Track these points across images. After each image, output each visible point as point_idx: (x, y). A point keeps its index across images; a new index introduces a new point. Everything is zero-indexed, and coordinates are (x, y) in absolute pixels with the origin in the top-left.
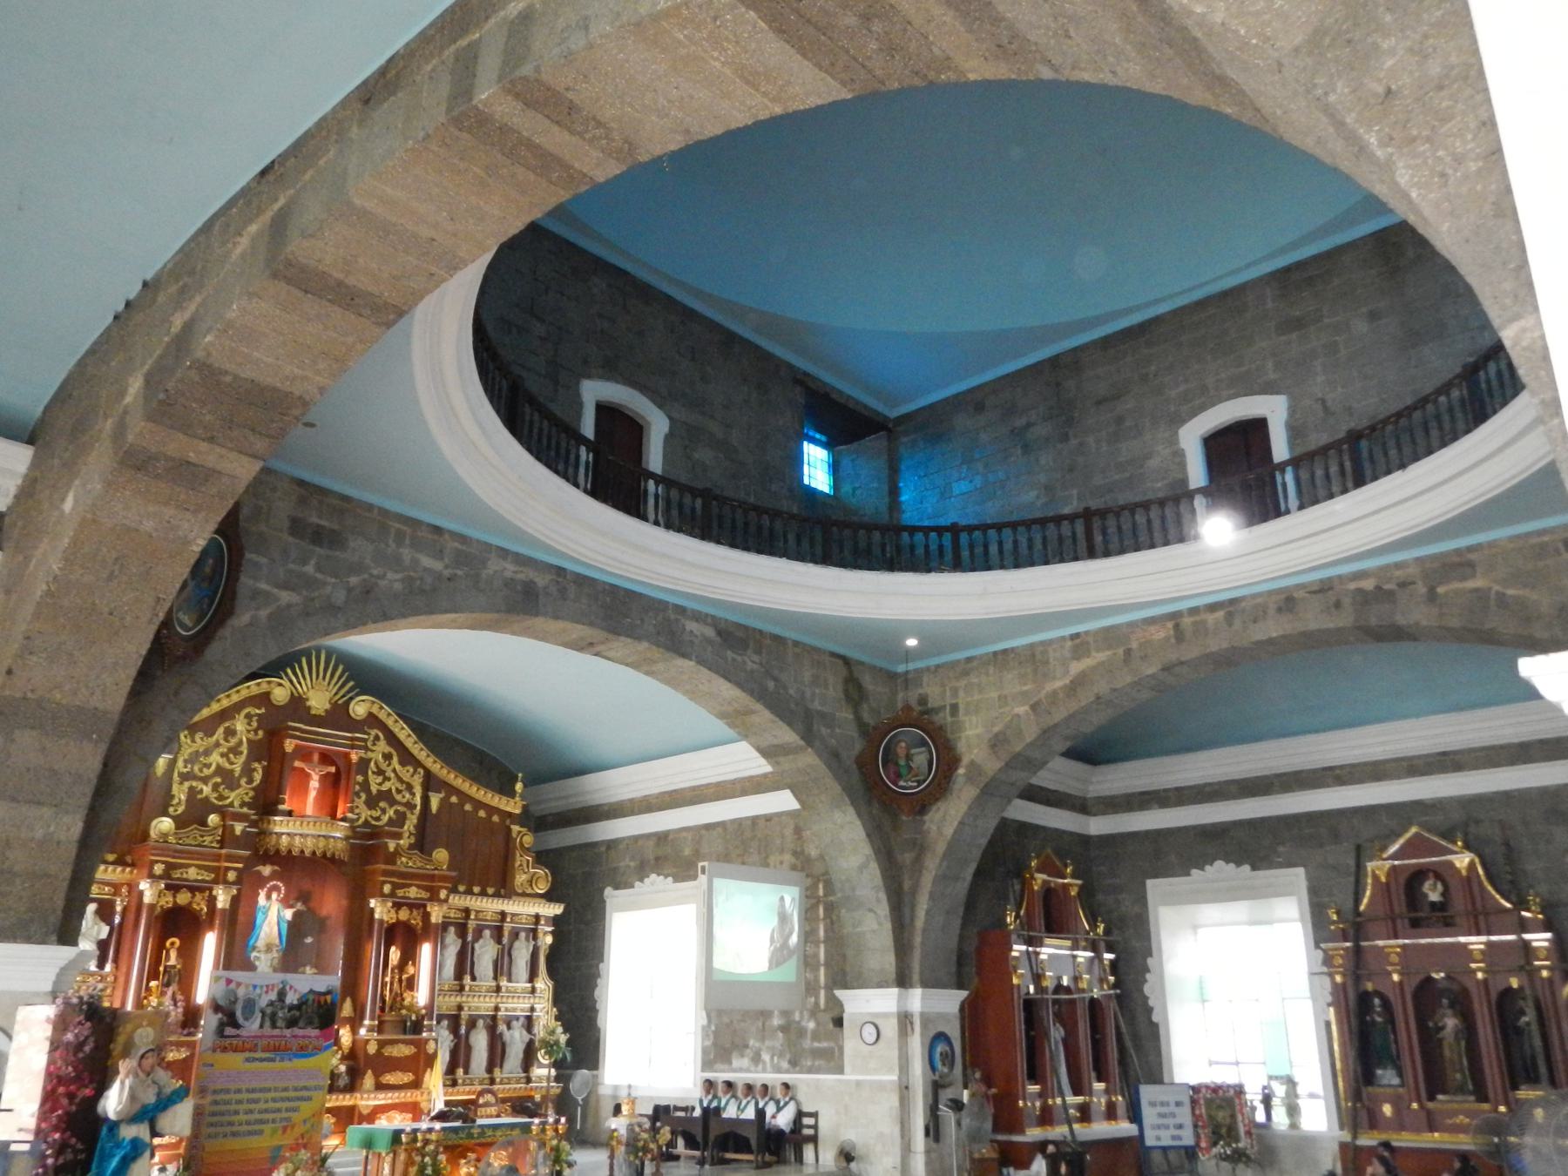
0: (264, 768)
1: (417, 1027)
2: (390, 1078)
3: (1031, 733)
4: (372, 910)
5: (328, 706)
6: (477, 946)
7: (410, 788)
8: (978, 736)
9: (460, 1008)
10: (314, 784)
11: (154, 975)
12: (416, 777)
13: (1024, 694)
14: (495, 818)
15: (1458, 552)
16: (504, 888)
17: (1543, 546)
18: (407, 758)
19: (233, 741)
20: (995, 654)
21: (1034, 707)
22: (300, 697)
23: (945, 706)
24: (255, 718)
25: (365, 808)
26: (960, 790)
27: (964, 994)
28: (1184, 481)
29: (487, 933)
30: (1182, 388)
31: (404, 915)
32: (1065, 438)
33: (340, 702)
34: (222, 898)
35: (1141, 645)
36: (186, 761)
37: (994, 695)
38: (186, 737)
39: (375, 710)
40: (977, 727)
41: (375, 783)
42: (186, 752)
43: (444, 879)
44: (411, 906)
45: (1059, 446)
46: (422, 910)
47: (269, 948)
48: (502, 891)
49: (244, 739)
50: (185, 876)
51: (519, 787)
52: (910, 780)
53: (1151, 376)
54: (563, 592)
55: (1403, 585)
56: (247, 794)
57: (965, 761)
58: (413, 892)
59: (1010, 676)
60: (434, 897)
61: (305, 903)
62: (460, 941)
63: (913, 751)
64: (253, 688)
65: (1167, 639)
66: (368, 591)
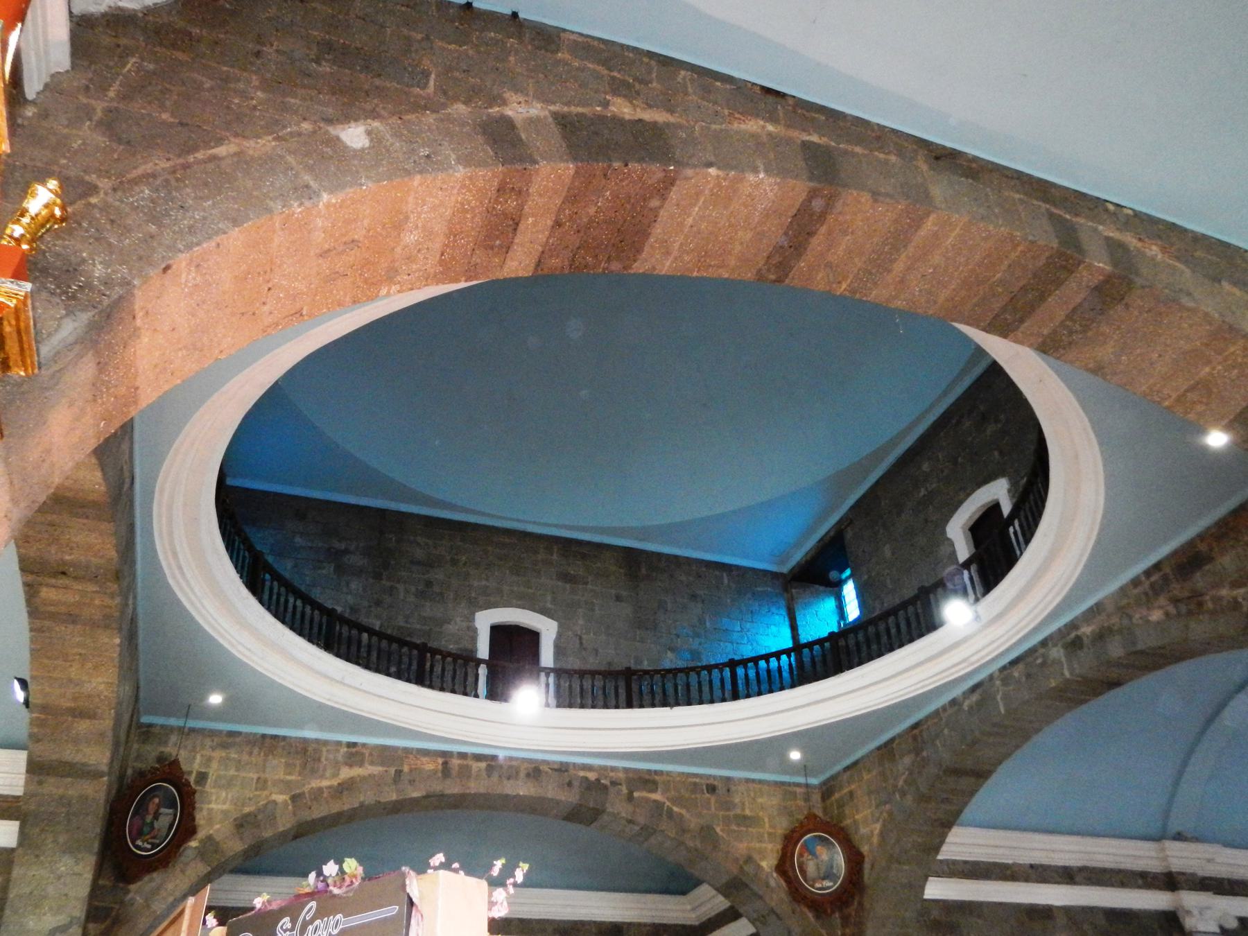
3: (285, 823)
8: (222, 811)
13: (288, 784)
15: (649, 772)
17: (695, 784)
20: (264, 736)
21: (294, 798)
23: (192, 772)
26: (187, 864)
28: (474, 651)
30: (484, 583)
32: (378, 577)
35: (411, 770)
37: (255, 776)
40: (224, 803)
45: (371, 581)
52: (147, 841)
53: (461, 564)
55: (614, 783)
57: (201, 834)
59: (275, 762)
63: (163, 810)
65: (435, 772)
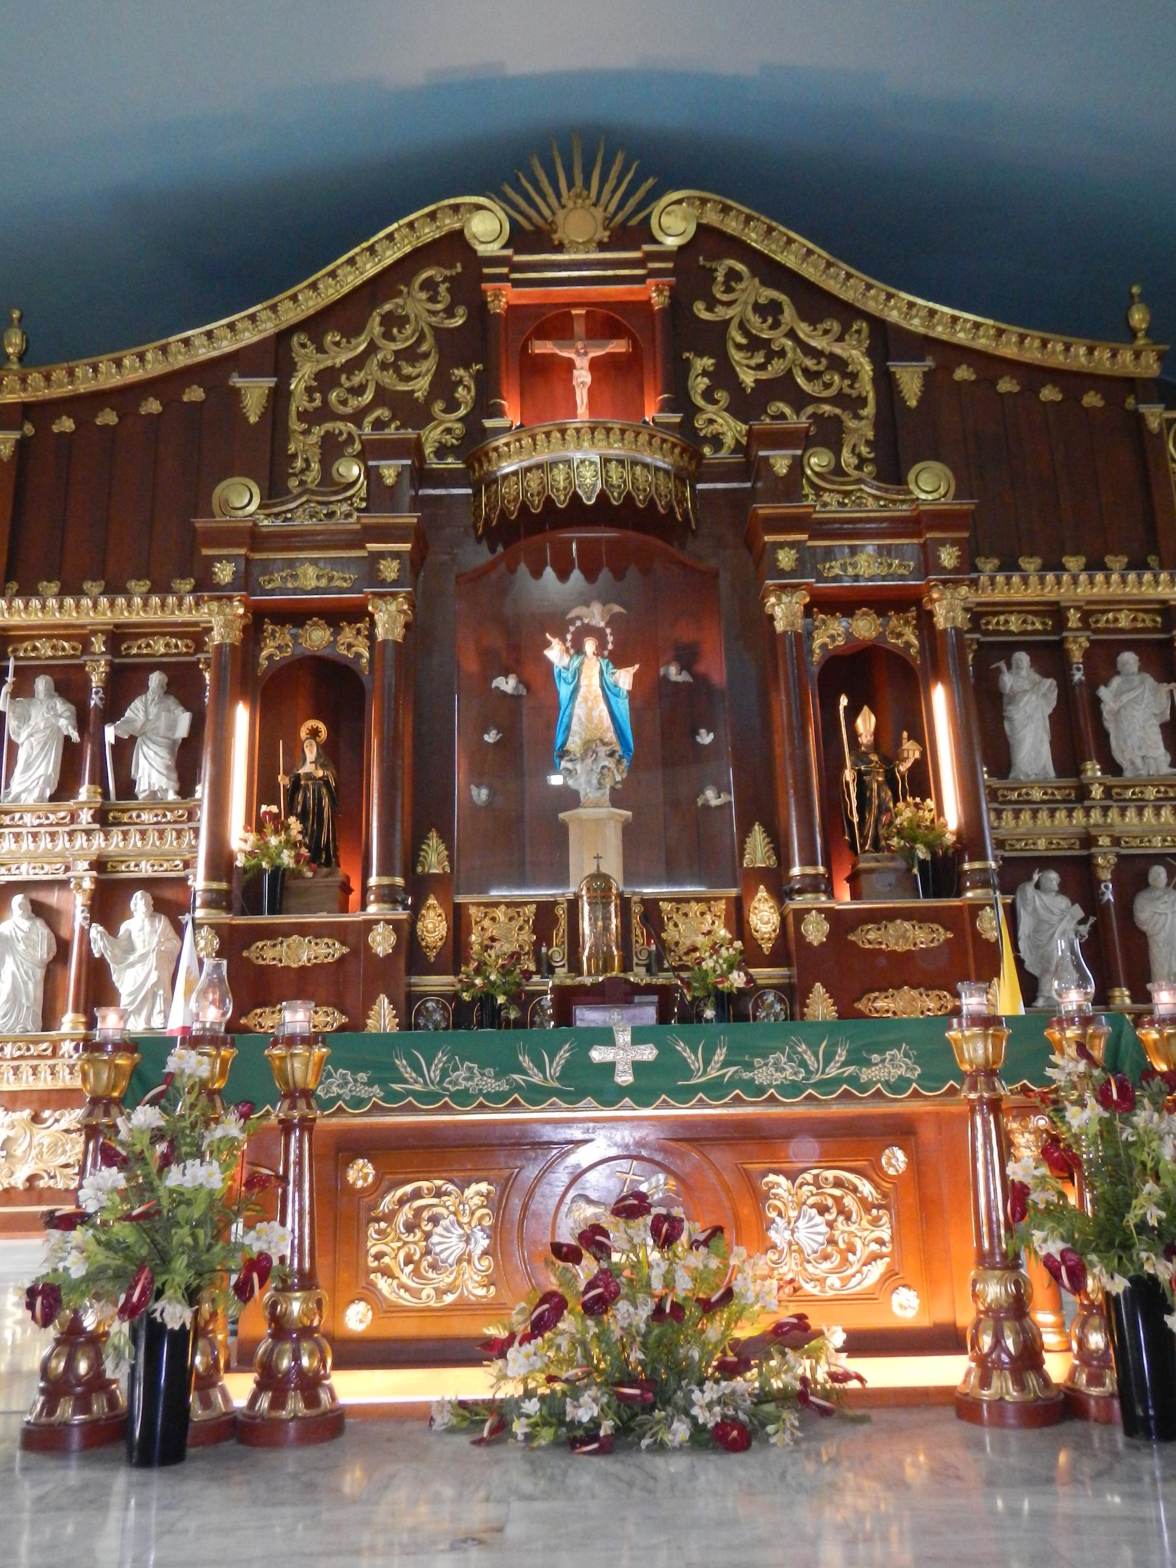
0: (478, 378)
2: (883, 1004)
4: (771, 618)
5: (605, 235)
6: (1103, 692)
7: (838, 364)
9: (1088, 840)
10: (582, 376)
12: (850, 339)
16: (1158, 555)
22: (538, 230)
24: (442, 288)
25: (731, 420)
29: (1129, 659)
31: (865, 627)
33: (634, 222)
36: (309, 390)
38: (304, 346)
39: (712, 217)
43: (939, 519)
46: (912, 613)
47: (589, 747)
48: (1152, 560)
49: (426, 330)
50: (290, 585)
51: (1138, 317)
56: (448, 431)
61: (685, 666)
62: (1049, 685)
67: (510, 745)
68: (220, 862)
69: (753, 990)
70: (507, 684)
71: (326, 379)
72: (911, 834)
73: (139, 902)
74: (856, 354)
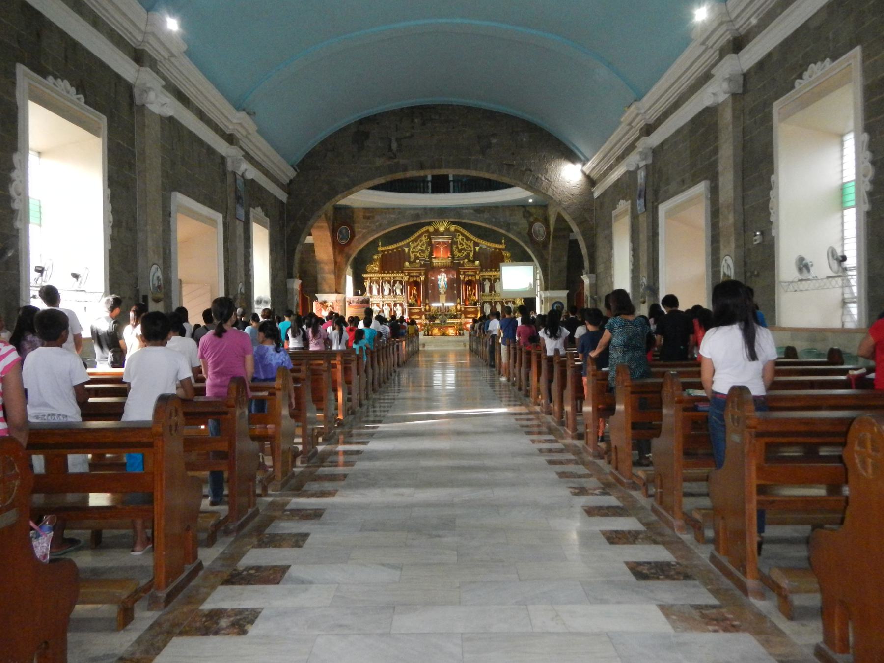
1: (475, 304)
2: (469, 316)
7: (470, 246)
10: (442, 250)
11: (411, 295)
14: (498, 250)
18: (468, 239)
19: (422, 242)
27: (568, 291)
31: (470, 278)
34: (423, 278)
39: (457, 228)
41: (460, 246)
42: (412, 247)
43: (477, 269)
44: (472, 276)
47: (442, 288)
51: (503, 241)
54: (426, 213)
58: (470, 273)
60: (476, 273)
64: (424, 229)
66: (380, 225)
67: (433, 285)
68: (408, 302)
69: (457, 315)
70: (433, 278)
71: (414, 248)
72: (472, 300)
73: (398, 305)
74: (472, 244)
